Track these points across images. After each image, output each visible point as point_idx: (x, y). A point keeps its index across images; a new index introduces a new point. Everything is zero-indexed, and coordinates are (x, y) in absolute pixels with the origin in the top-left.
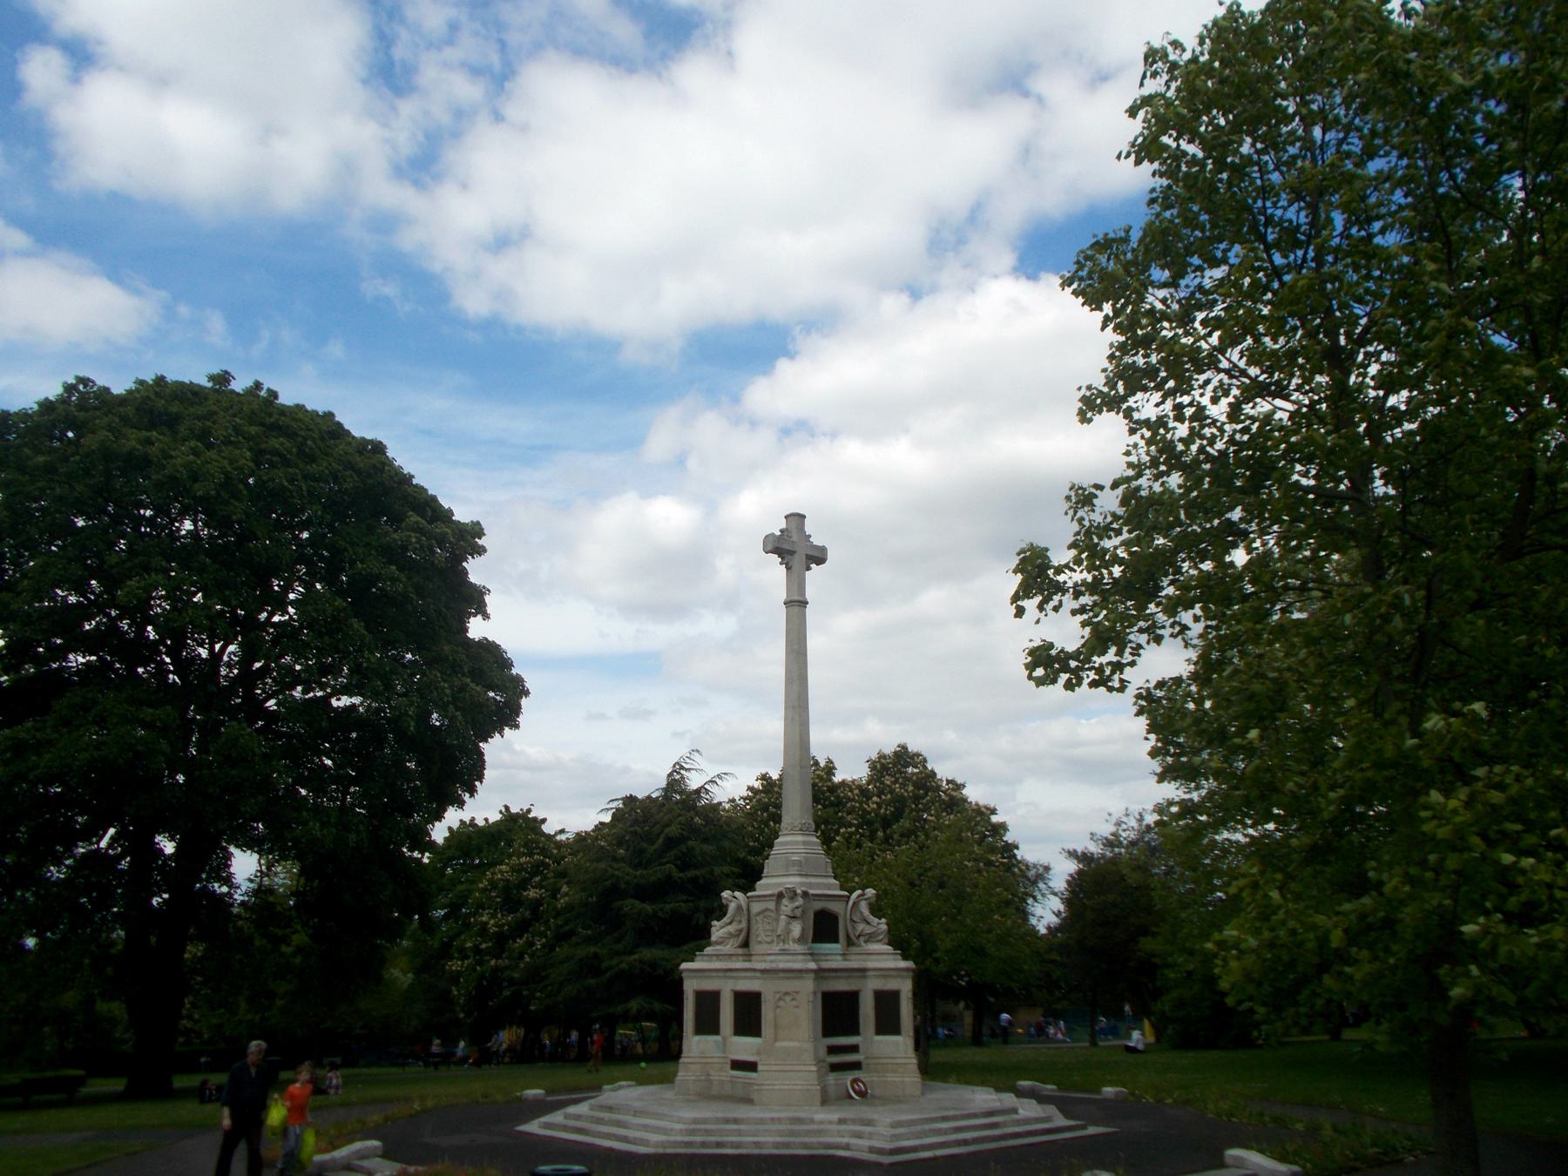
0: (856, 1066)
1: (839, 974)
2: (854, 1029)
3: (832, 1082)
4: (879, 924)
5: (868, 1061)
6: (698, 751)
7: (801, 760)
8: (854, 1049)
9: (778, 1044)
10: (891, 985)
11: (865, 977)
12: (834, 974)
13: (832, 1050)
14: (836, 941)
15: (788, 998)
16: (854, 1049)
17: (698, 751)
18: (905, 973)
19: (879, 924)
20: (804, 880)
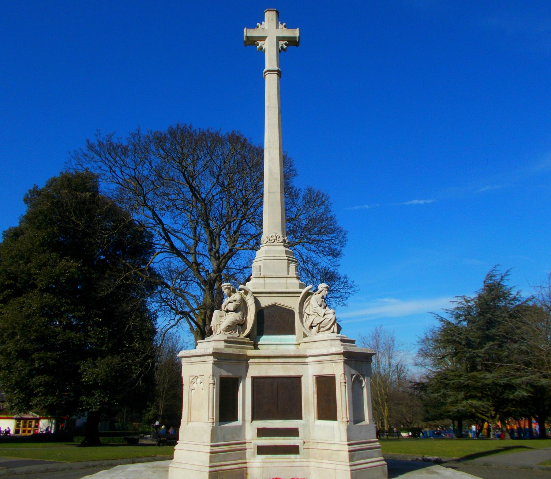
0: (294, 450)
1: (272, 360)
2: (299, 416)
3: (259, 464)
4: (325, 314)
5: (306, 445)
6: (498, 265)
7: (269, 189)
8: (294, 432)
9: (190, 424)
10: (327, 370)
11: (305, 363)
12: (266, 360)
13: (262, 432)
14: (291, 331)
15: (198, 380)
16: (294, 432)
17: (498, 265)
18: (337, 357)
19: (325, 314)
20: (261, 281)
